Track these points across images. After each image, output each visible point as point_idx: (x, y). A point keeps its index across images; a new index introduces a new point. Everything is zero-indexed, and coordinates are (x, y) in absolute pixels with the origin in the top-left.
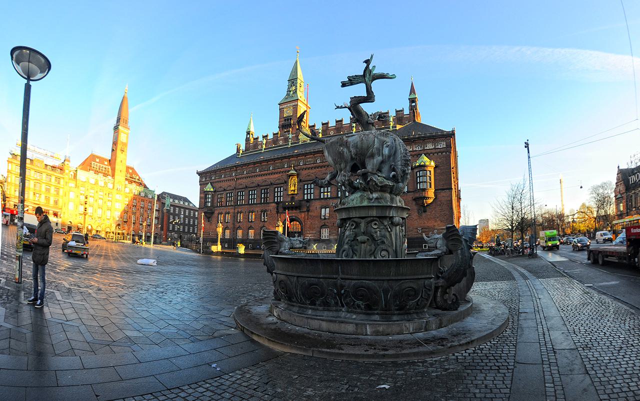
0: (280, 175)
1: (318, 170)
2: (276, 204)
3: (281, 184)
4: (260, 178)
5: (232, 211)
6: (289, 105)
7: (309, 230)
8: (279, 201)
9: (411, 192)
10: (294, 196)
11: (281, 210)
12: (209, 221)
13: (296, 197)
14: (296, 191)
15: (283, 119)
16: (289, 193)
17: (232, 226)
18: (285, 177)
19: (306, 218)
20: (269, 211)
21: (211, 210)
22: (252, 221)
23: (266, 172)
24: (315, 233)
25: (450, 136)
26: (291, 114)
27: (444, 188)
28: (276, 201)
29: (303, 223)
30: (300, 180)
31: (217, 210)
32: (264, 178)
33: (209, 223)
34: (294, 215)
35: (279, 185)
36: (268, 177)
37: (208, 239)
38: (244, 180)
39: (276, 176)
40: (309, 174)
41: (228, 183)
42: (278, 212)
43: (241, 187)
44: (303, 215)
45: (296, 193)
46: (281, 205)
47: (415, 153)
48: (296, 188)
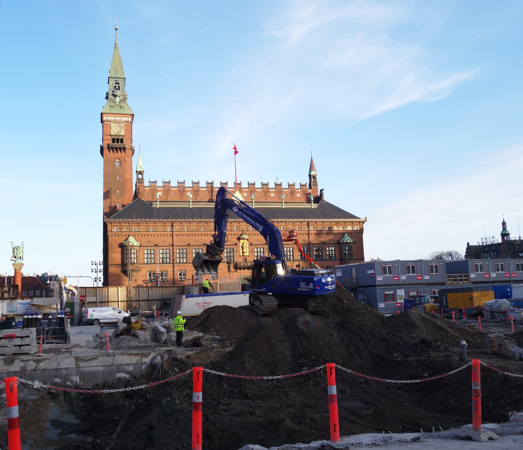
2: (228, 264)
6: (117, 119)
9: (338, 260)
11: (232, 269)
14: (248, 253)
15: (110, 138)
21: (138, 267)
26: (123, 133)
27: (359, 258)
30: (251, 244)
31: (144, 267)
38: (185, 238)
41: (163, 239)
42: (229, 271)
43: (181, 244)
45: (248, 255)
48: (248, 251)
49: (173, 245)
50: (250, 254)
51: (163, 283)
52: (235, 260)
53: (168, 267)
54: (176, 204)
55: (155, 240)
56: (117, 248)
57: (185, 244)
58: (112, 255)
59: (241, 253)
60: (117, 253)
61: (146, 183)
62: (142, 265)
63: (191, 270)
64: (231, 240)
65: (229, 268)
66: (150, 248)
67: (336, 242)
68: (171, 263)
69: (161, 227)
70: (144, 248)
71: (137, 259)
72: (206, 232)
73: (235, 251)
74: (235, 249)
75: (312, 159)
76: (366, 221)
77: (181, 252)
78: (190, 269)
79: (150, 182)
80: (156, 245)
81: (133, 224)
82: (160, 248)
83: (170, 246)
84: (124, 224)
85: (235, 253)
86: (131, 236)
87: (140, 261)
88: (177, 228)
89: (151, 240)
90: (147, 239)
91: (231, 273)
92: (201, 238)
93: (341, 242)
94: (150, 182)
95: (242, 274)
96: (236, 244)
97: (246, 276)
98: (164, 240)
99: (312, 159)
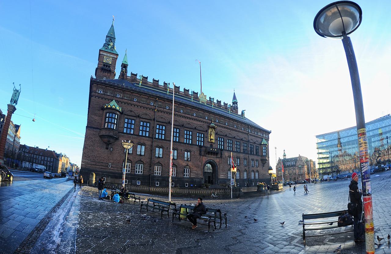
0: (202, 123)
1: (226, 130)
3: (203, 131)
4: (184, 119)
5: (148, 143)
7: (222, 171)
8: (200, 145)
10: (213, 144)
11: (203, 153)
12: (107, 149)
13: (214, 145)
16: (209, 141)
17: (148, 160)
18: (205, 126)
19: (220, 162)
20: (193, 152)
22: (141, 155)
23: (189, 116)
24: (225, 174)
25: (268, 133)
28: (200, 145)
29: (218, 166)
31: (123, 136)
32: (188, 120)
33: (107, 151)
34: (212, 159)
35: (200, 131)
36: (191, 121)
37: (104, 172)
39: (199, 123)
40: (221, 131)
41: (145, 111)
42: (200, 154)
44: (218, 160)
45: (214, 142)
46: (203, 149)
47: (261, 137)
49: (154, 120)
50: (215, 142)
51: (140, 157)
52: (205, 145)
53: (147, 140)
54: (156, 88)
55: (137, 111)
56: (99, 110)
57: (164, 121)
58: (92, 116)
59: (209, 139)
60: (96, 116)
61: (129, 74)
62: (121, 134)
63: (168, 148)
64: (203, 127)
65: (200, 152)
66: (131, 117)
67: (259, 143)
68: (150, 138)
69: (145, 100)
70: (126, 116)
71: (117, 126)
72: (184, 114)
73: (205, 137)
74: (205, 135)
75: (234, 93)
76: (271, 133)
77: (161, 128)
78: (167, 146)
79: (132, 74)
80: (139, 116)
81: (118, 90)
82: (141, 119)
83: (151, 120)
84: (109, 88)
85: (205, 139)
86: (114, 100)
87: (120, 129)
88: (160, 104)
89: (133, 110)
90: (129, 108)
91: (201, 157)
92: (179, 119)
93: (263, 143)
94: (132, 74)
95: (209, 159)
96: (207, 131)
97: (212, 161)
98: (146, 113)
99: (234, 93)
